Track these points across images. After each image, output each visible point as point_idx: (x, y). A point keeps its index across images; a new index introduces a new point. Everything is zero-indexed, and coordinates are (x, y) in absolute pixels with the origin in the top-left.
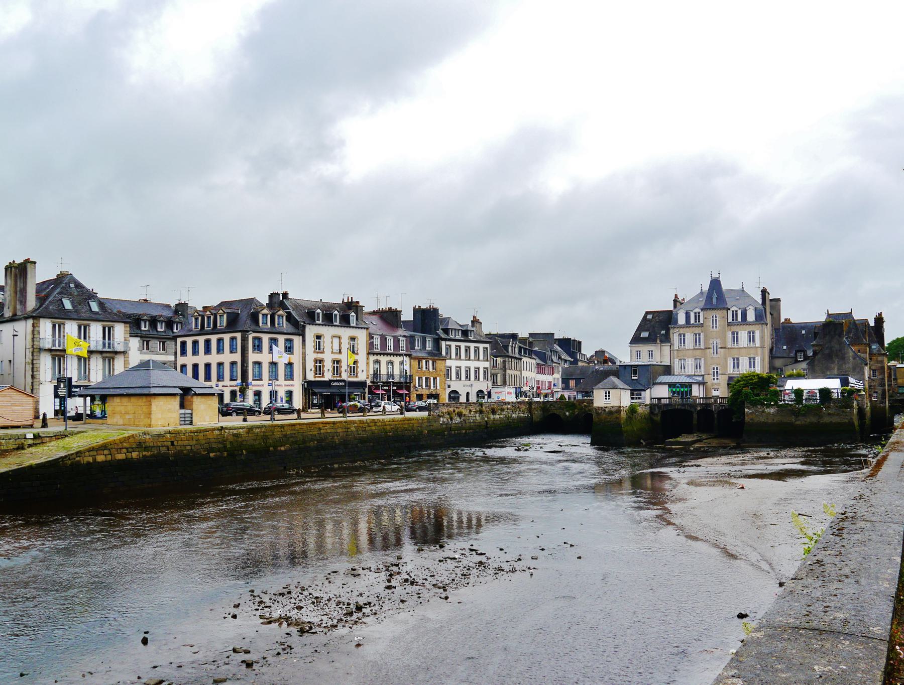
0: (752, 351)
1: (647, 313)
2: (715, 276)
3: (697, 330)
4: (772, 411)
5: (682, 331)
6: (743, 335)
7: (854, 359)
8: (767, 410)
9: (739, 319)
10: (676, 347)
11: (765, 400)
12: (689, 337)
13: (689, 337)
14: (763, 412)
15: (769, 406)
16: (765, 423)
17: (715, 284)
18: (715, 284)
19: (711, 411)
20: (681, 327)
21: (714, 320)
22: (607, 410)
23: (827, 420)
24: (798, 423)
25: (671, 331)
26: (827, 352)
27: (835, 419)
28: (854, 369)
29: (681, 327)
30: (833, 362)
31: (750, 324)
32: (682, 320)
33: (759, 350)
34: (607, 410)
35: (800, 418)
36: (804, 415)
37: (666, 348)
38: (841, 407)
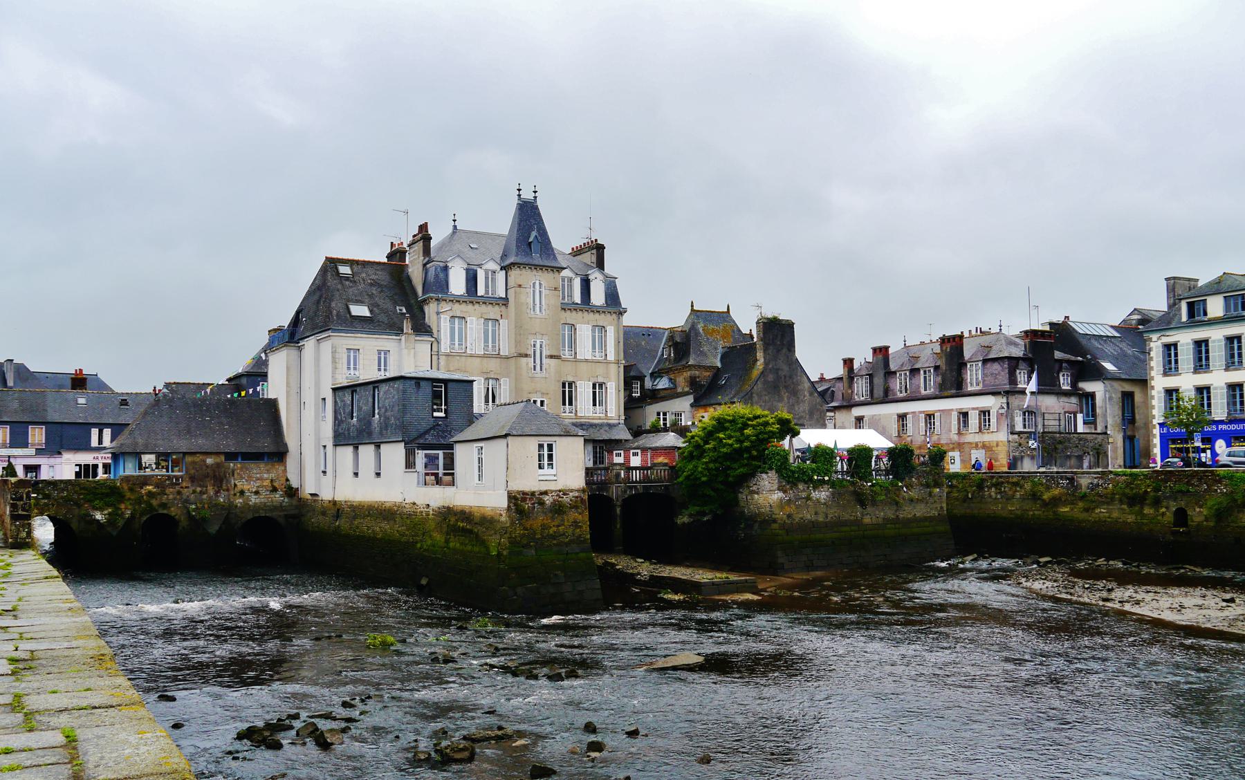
0: (600, 369)
1: (331, 264)
2: (527, 195)
3: (493, 312)
4: (822, 494)
5: (458, 309)
6: (585, 332)
7: (811, 394)
8: (815, 495)
9: (577, 298)
10: (445, 347)
11: (813, 471)
12: (474, 325)
13: (474, 325)
14: (808, 498)
15: (818, 485)
16: (814, 525)
17: (528, 214)
18: (528, 214)
19: (610, 499)
20: (457, 300)
21: (537, 292)
22: (548, 500)
23: (908, 512)
24: (867, 520)
25: (430, 310)
26: (771, 378)
27: (920, 511)
28: (811, 413)
29: (457, 300)
30: (781, 400)
31: (597, 310)
32: (457, 284)
33: (613, 369)
34: (548, 500)
35: (869, 509)
36: (874, 503)
37: (423, 347)
38: (928, 486)
